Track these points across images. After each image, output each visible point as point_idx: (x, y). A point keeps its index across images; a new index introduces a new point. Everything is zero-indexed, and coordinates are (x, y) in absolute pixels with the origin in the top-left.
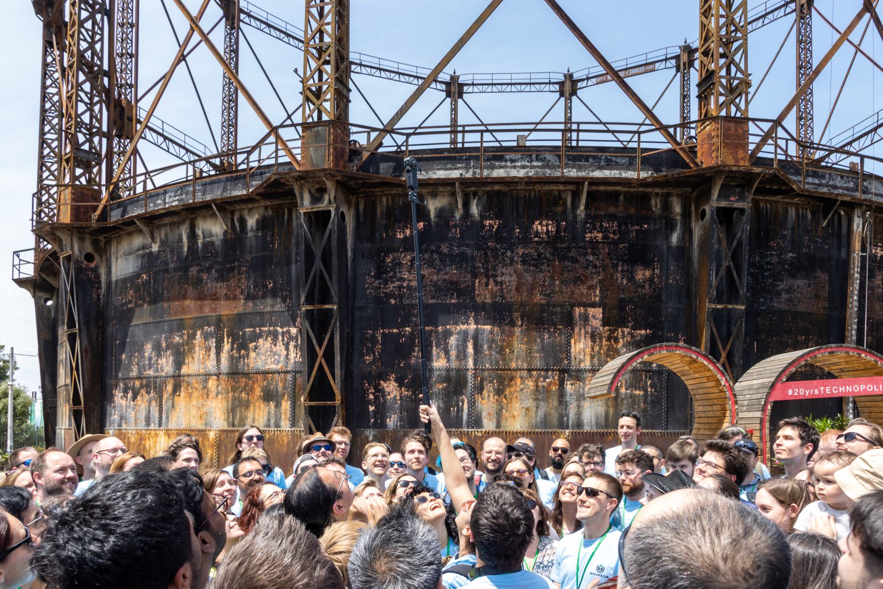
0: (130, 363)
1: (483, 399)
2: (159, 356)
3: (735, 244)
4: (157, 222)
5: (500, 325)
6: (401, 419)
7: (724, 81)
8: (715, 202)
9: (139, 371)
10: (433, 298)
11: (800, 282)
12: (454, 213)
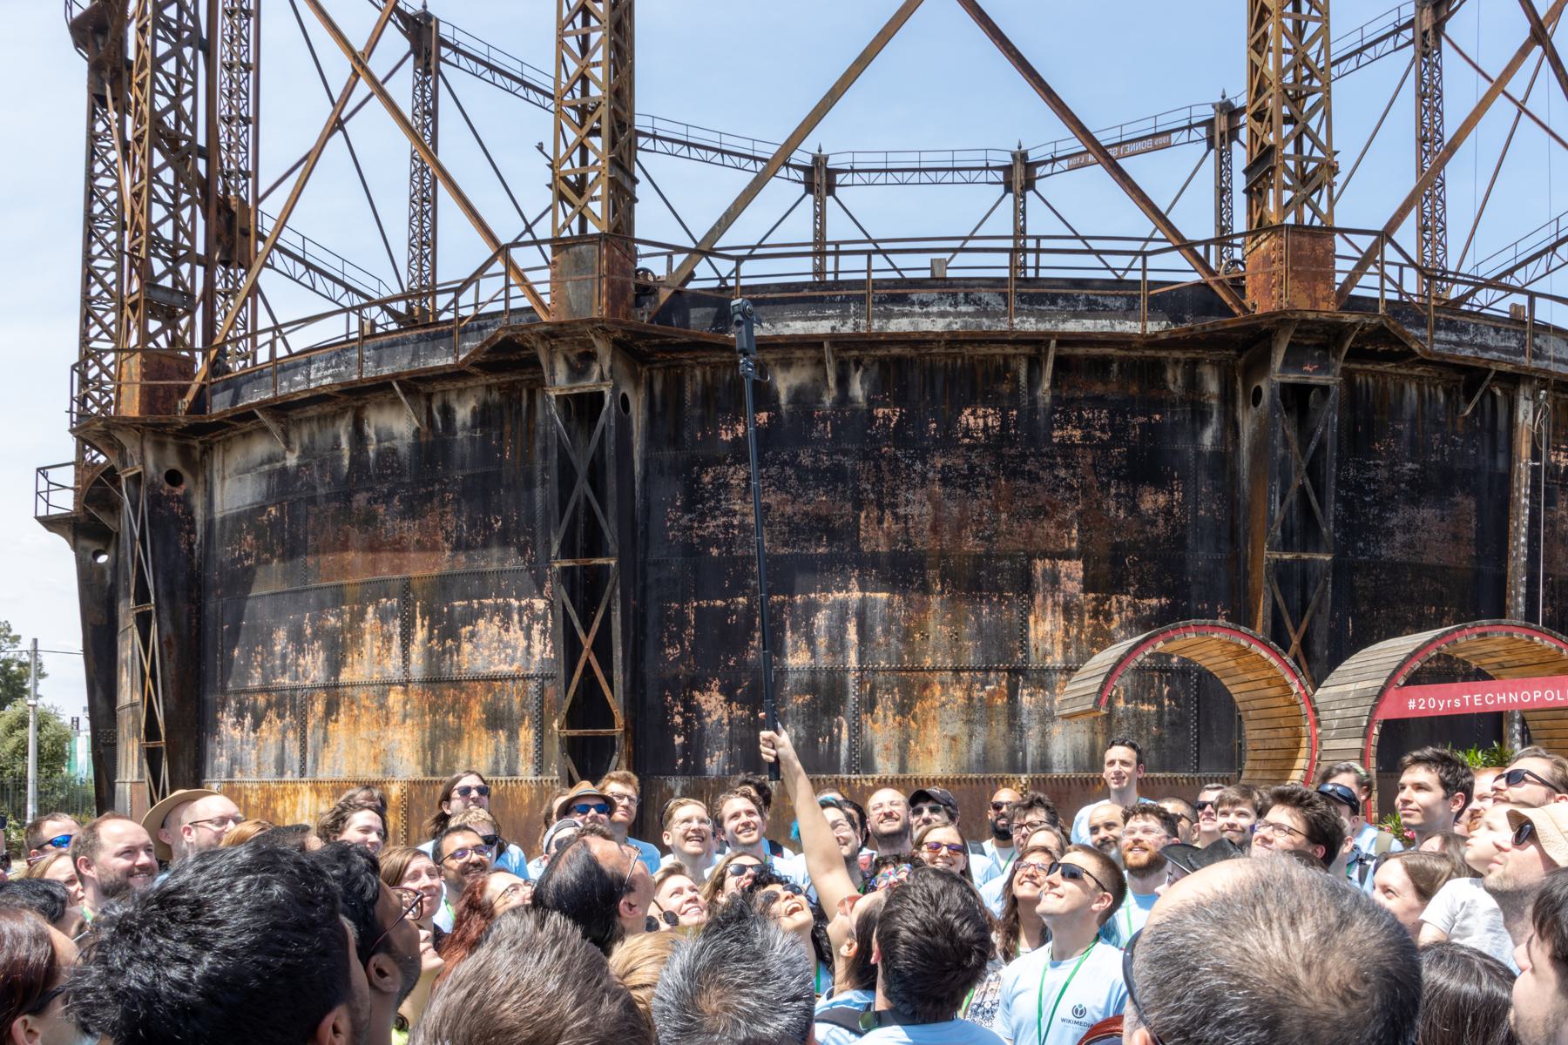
0: (248, 665)
1: (875, 722)
2: (300, 651)
3: (1312, 448)
4: (294, 414)
6: (731, 758)
7: (1291, 164)
8: (1278, 373)
9: (265, 677)
10: (785, 544)
11: (1427, 513)
12: (821, 395)
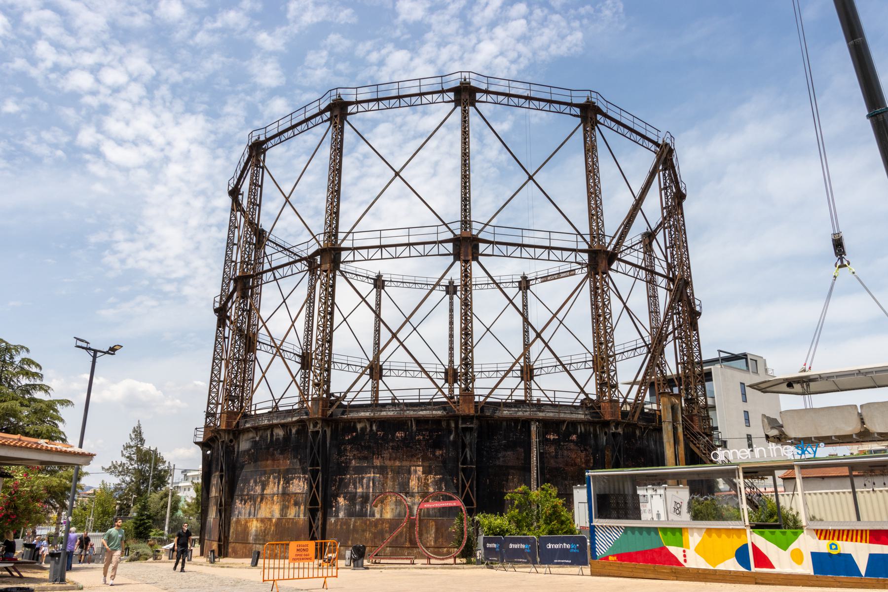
5: (383, 474)
